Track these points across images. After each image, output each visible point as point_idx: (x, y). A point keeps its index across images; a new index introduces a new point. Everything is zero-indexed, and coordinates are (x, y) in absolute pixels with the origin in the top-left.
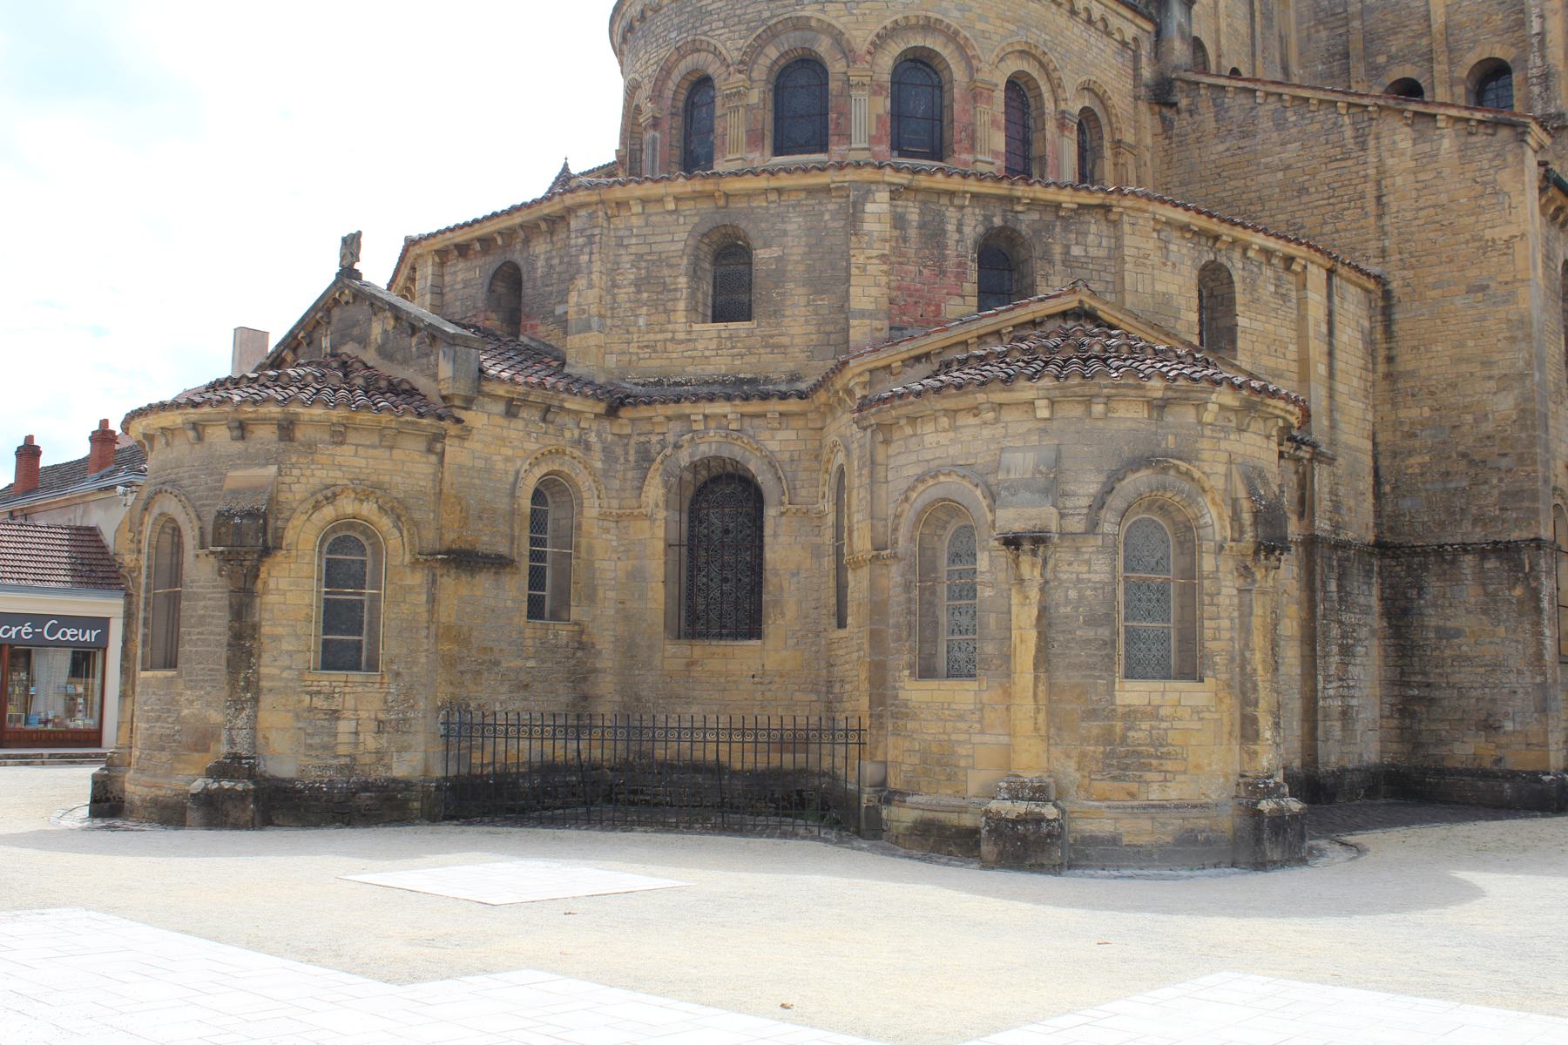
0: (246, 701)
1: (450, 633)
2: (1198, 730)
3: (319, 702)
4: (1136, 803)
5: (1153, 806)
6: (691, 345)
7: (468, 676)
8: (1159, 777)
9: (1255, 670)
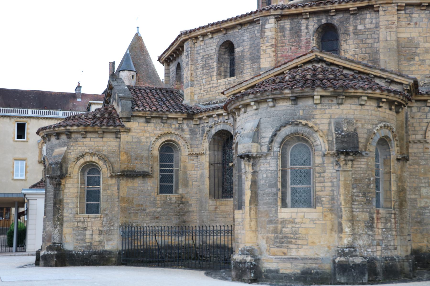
0: (58, 225)
1: (122, 200)
2: (313, 228)
3: (80, 225)
4: (286, 257)
5: (292, 258)
6: (218, 88)
7: (132, 215)
8: (295, 246)
9: (341, 203)
